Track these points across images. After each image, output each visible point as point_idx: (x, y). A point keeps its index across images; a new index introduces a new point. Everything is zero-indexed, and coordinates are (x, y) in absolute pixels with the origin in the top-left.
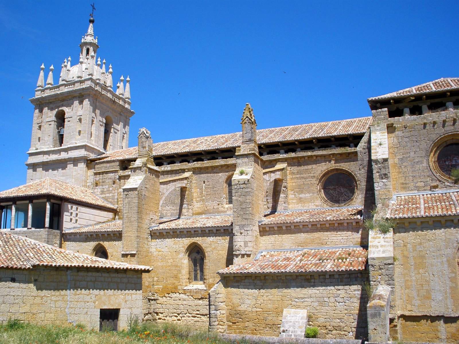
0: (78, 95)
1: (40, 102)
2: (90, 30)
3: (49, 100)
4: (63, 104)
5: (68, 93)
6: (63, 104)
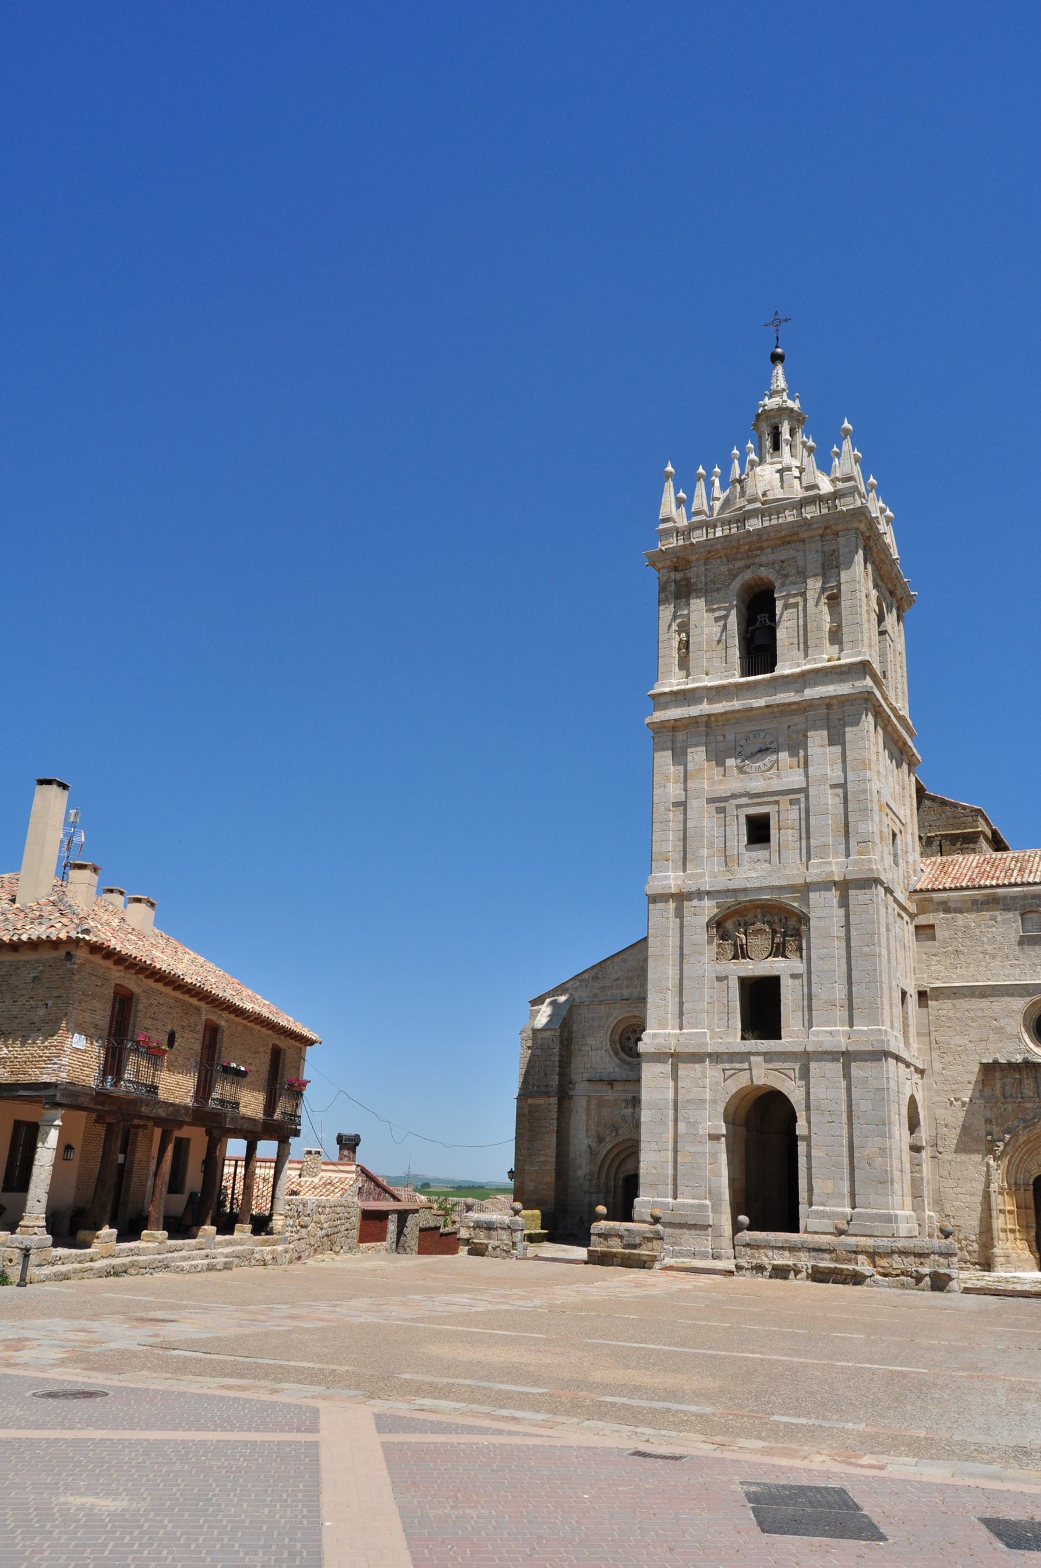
2: (779, 378)
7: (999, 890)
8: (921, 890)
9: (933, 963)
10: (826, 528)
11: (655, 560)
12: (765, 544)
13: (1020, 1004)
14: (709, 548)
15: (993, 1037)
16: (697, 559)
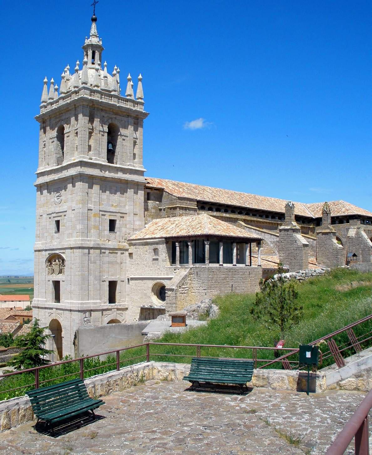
0: (135, 116)
1: (93, 105)
2: (94, 29)
3: (103, 107)
4: (116, 117)
5: (126, 110)
6: (116, 117)
7: (148, 241)
8: (130, 240)
9: (132, 268)
10: (75, 105)
11: (37, 119)
12: (62, 112)
13: (151, 284)
14: (49, 115)
15: (144, 297)
16: (48, 119)
